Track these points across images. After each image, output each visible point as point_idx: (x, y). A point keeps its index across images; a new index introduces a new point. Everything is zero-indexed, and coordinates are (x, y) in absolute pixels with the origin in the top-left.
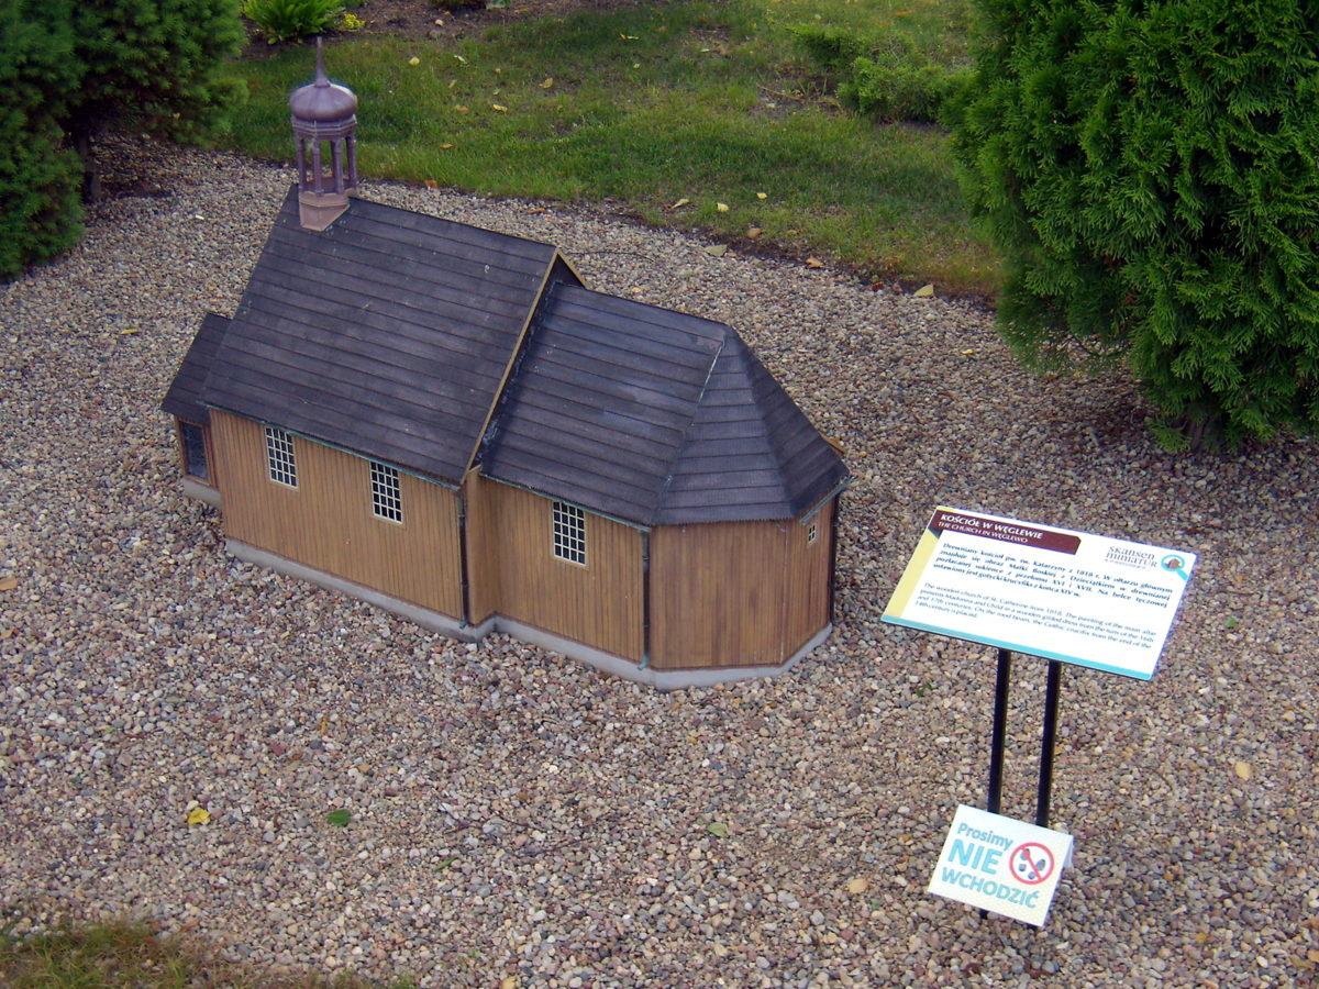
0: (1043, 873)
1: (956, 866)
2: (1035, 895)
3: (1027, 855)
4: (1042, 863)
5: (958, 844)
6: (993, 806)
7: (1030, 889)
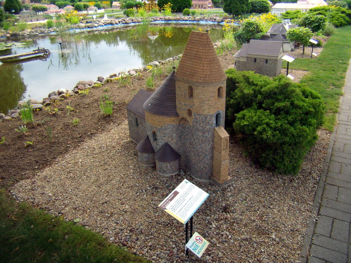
1: (197, 251)
3: (198, 240)
7: (203, 242)
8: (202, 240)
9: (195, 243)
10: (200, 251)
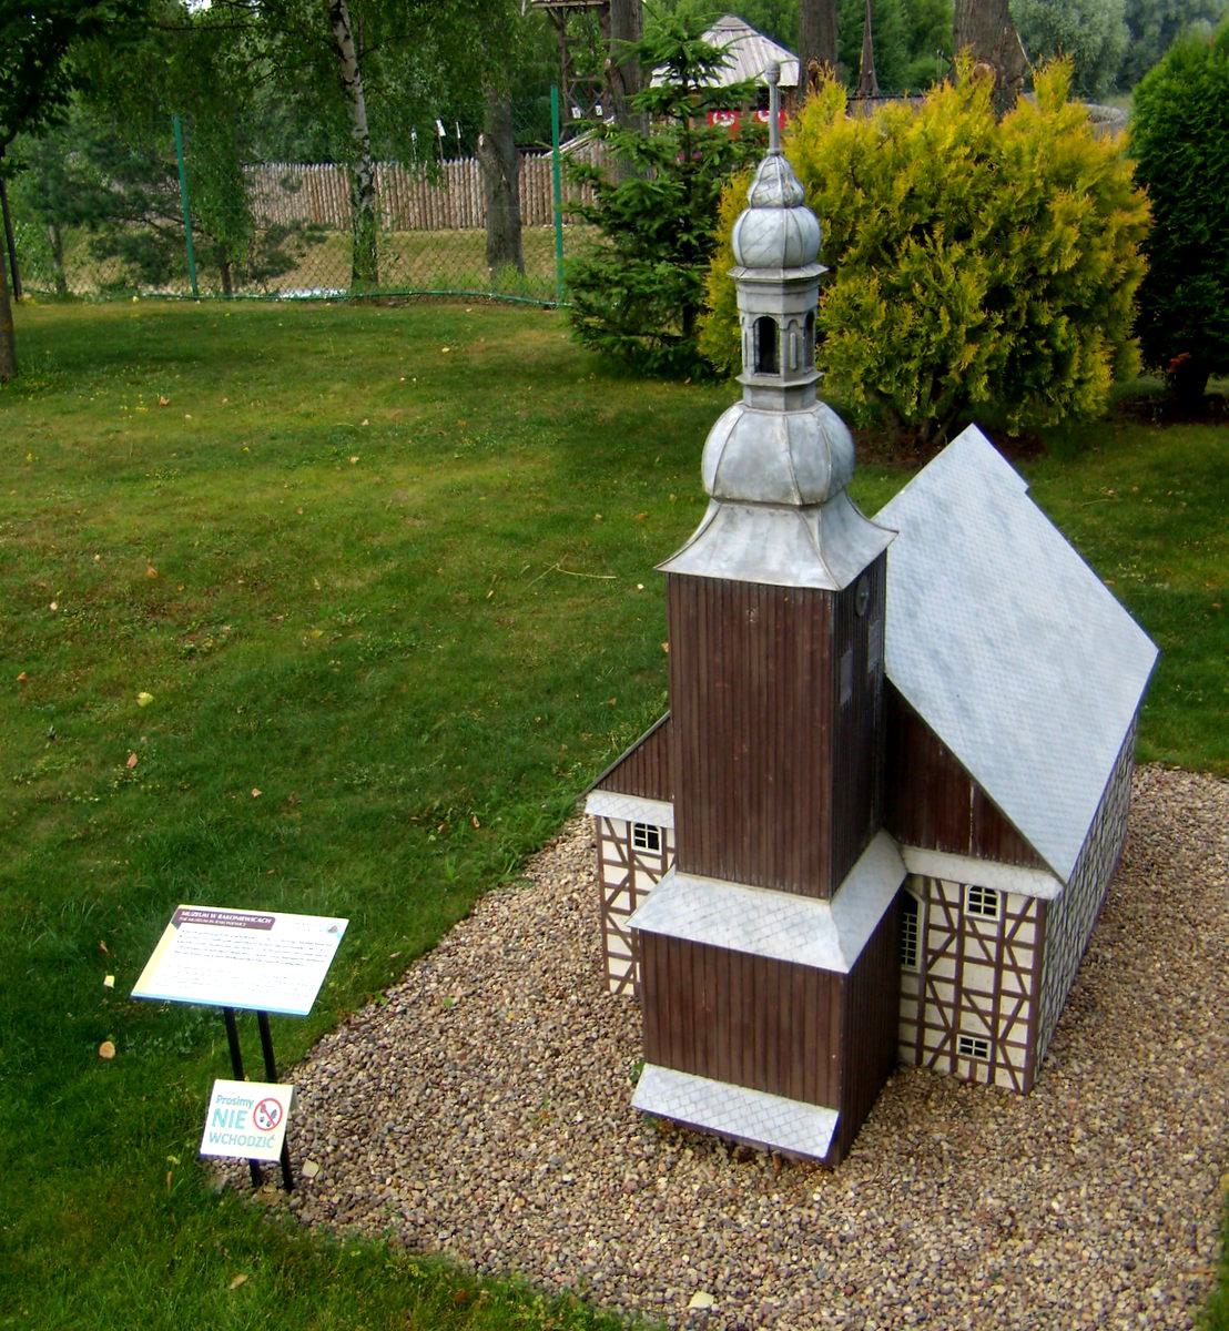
3: (264, 1110)
5: (217, 1112)
6: (239, 1076)
9: (245, 1108)
10: (227, 1139)
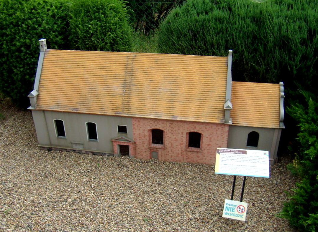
0: (243, 211)
1: (227, 211)
2: (243, 215)
3: (240, 208)
4: (243, 209)
5: (227, 207)
7: (242, 214)
8: (243, 212)
10: (230, 214)
